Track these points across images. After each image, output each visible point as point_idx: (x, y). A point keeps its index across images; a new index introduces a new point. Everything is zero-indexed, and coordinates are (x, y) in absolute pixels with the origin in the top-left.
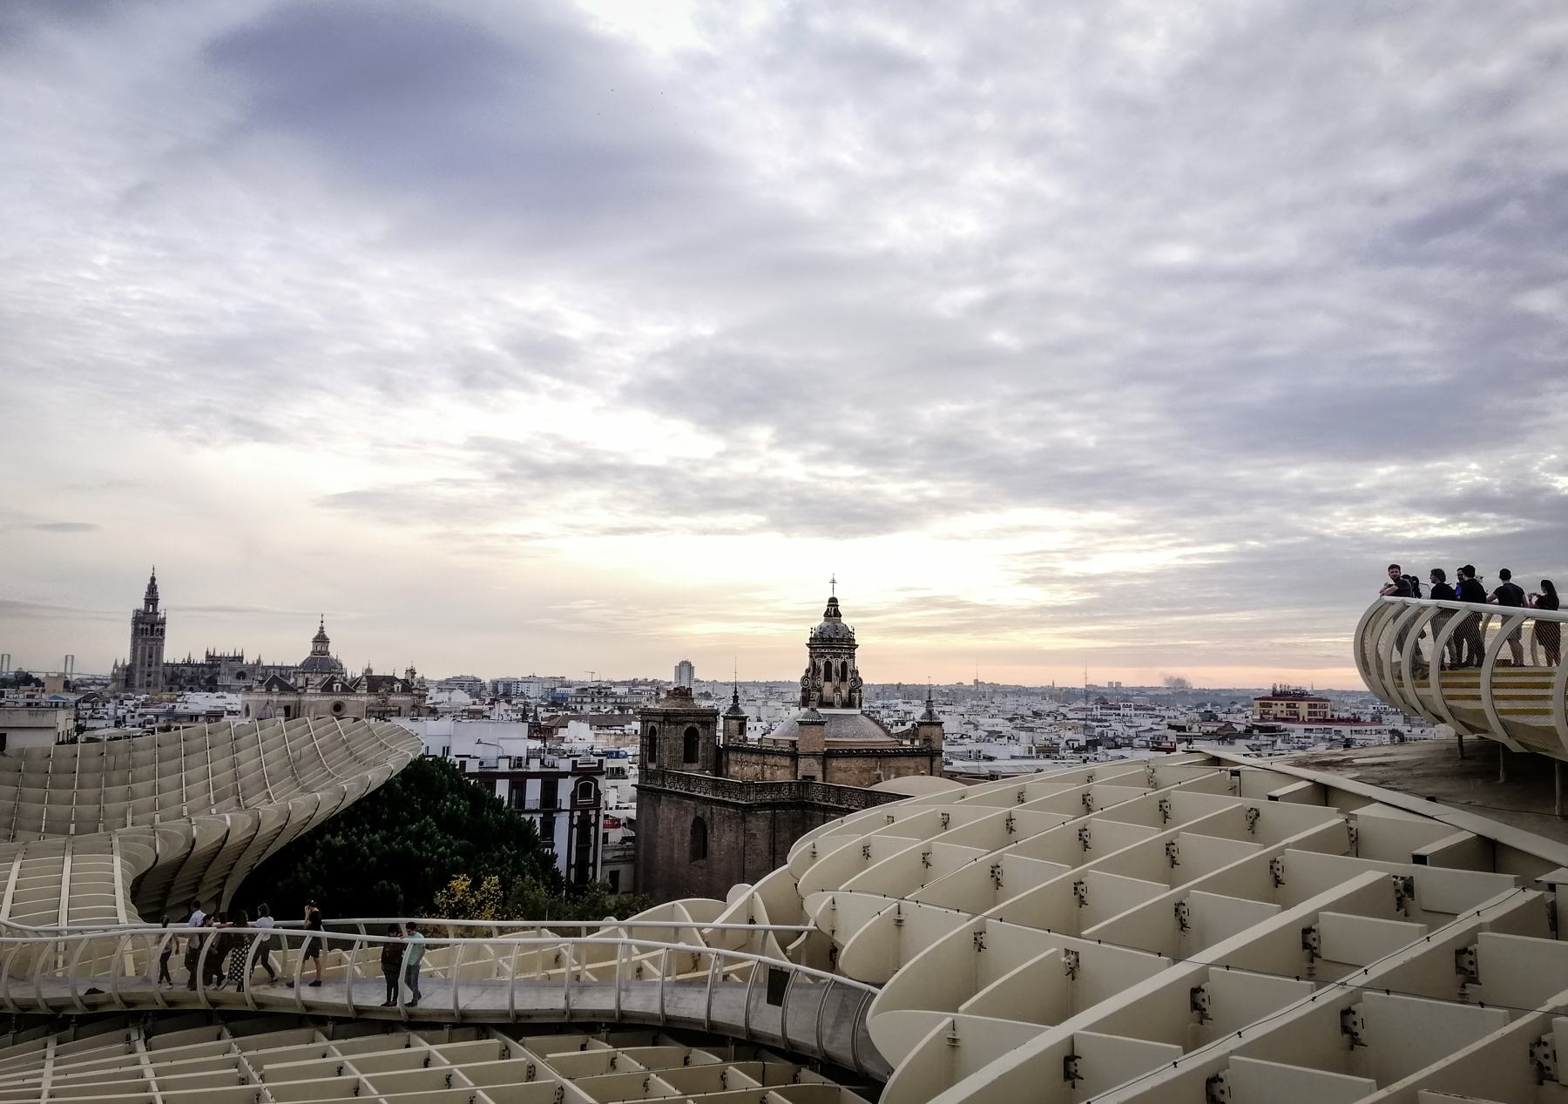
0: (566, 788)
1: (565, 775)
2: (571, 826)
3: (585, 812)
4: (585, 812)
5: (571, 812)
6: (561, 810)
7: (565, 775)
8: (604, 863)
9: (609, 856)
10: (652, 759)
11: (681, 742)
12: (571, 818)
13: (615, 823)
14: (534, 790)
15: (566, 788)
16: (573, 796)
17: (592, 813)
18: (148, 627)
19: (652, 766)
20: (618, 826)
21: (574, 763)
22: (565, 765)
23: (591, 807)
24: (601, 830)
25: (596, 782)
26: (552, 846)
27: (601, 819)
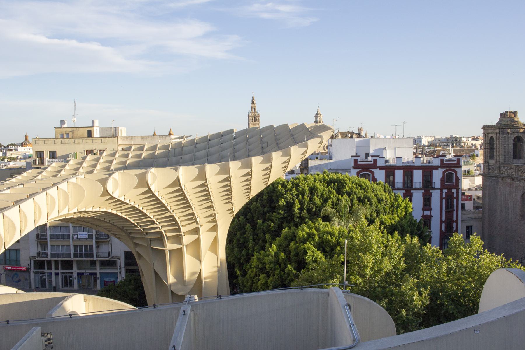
0: (437, 176)
1: (436, 168)
2: (442, 198)
3: (450, 189)
4: (450, 189)
5: (441, 190)
6: (434, 189)
7: (436, 168)
8: (462, 221)
9: (465, 217)
10: (492, 157)
11: (512, 146)
12: (441, 194)
13: (469, 198)
14: (418, 176)
15: (437, 176)
16: (442, 180)
17: (454, 191)
18: (253, 118)
19: (492, 162)
20: (471, 199)
21: (442, 161)
22: (436, 162)
23: (454, 187)
24: (460, 202)
25: (456, 172)
26: (430, 210)
27: (460, 195)
